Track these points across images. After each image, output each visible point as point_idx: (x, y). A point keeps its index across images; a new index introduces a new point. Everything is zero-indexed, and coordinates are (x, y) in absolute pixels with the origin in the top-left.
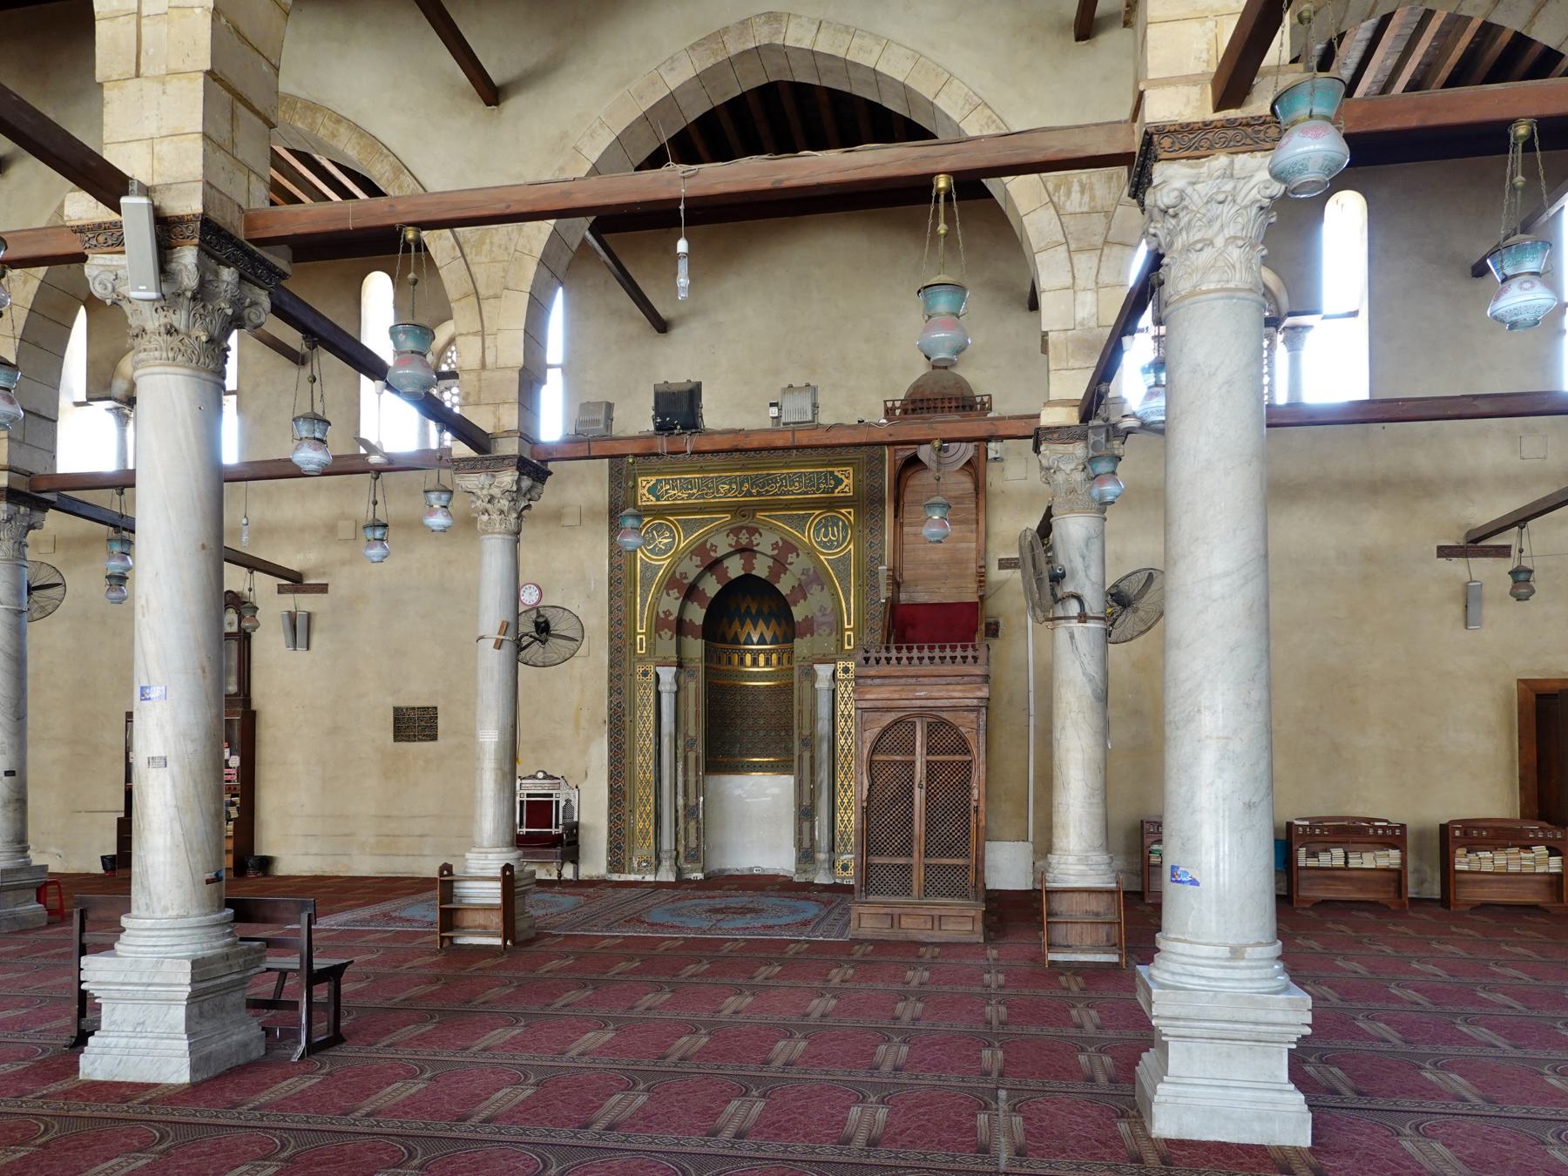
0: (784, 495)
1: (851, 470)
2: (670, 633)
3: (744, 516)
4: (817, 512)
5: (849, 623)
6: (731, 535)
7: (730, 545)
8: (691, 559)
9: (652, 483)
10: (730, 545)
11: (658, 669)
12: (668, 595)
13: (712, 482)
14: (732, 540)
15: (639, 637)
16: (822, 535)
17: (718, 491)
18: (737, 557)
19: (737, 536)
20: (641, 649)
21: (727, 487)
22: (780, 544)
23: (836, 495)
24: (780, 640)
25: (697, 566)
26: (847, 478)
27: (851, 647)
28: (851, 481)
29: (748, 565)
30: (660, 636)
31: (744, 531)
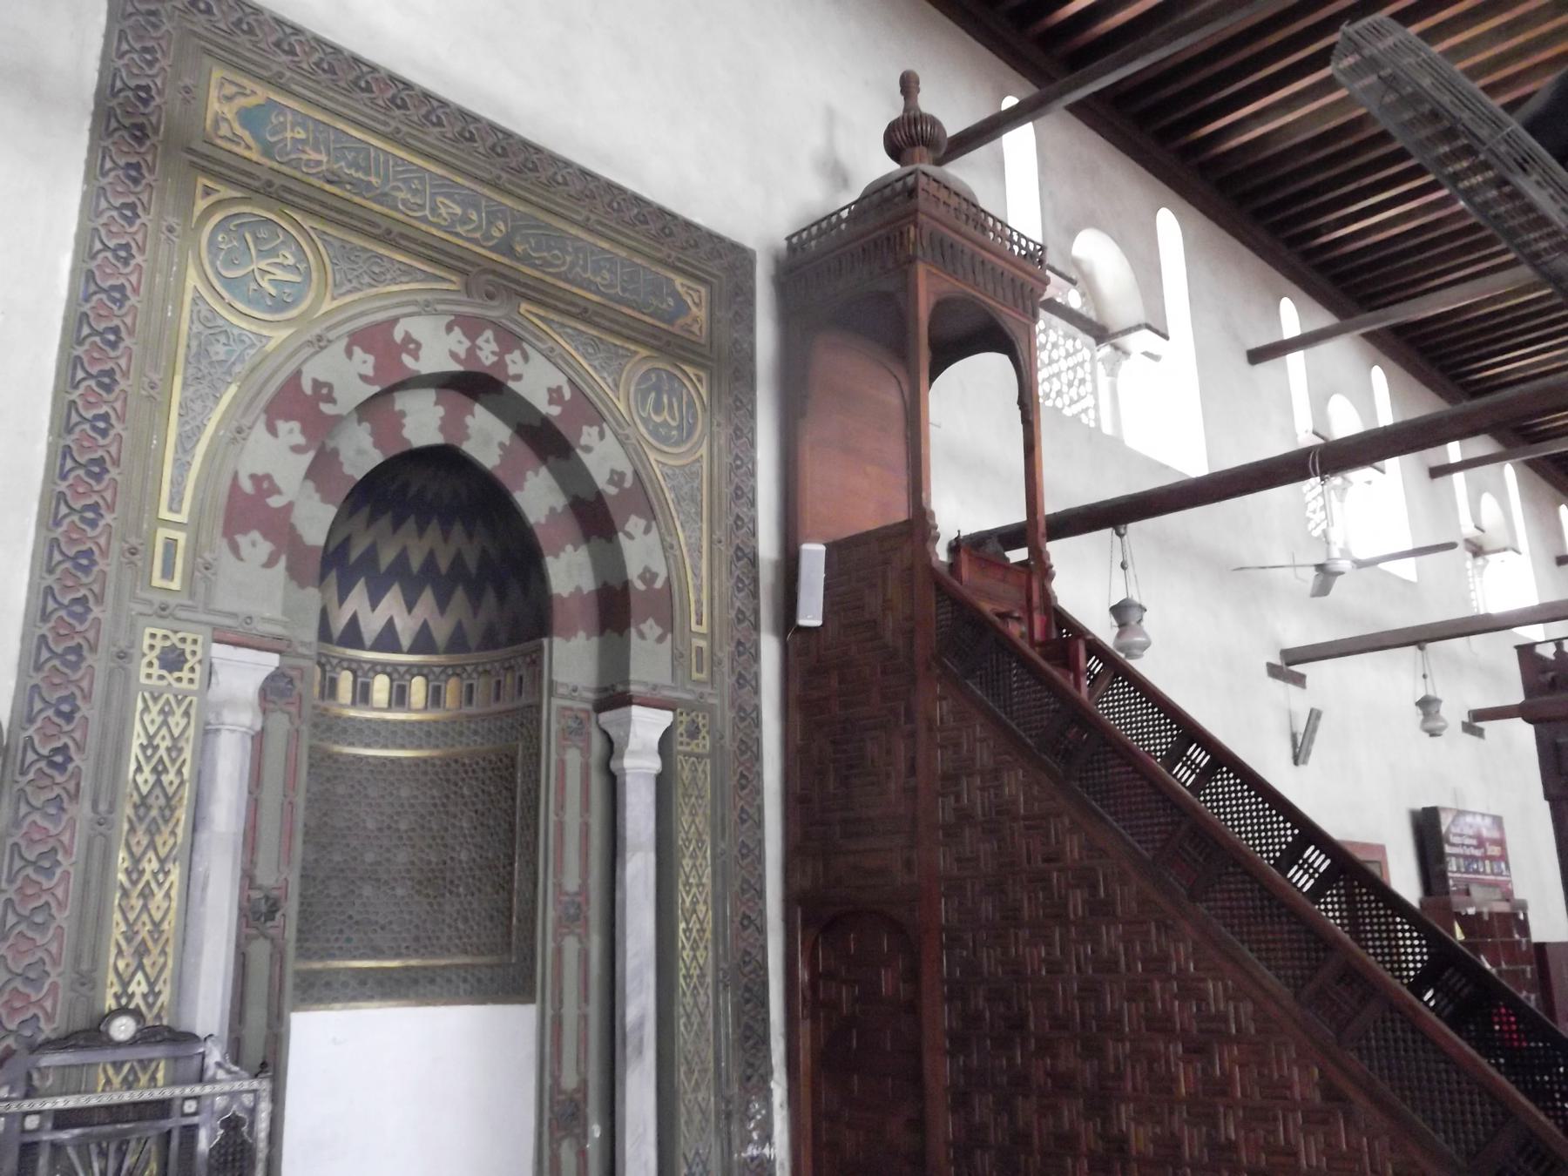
0: (581, 287)
1: (703, 290)
2: (265, 548)
3: (490, 296)
4: (644, 352)
5: (699, 622)
6: (457, 330)
7: (454, 355)
8: (349, 353)
9: (251, 101)
10: (454, 355)
11: (218, 651)
12: (272, 430)
13: (422, 180)
14: (457, 341)
15: (162, 534)
17: (434, 210)
18: (430, 395)
20: (168, 573)
21: (458, 210)
22: (567, 394)
23: (676, 330)
24: (406, 641)
25: (364, 378)
27: (704, 676)
28: (701, 313)
29: (452, 422)
30: (235, 549)
31: (489, 334)
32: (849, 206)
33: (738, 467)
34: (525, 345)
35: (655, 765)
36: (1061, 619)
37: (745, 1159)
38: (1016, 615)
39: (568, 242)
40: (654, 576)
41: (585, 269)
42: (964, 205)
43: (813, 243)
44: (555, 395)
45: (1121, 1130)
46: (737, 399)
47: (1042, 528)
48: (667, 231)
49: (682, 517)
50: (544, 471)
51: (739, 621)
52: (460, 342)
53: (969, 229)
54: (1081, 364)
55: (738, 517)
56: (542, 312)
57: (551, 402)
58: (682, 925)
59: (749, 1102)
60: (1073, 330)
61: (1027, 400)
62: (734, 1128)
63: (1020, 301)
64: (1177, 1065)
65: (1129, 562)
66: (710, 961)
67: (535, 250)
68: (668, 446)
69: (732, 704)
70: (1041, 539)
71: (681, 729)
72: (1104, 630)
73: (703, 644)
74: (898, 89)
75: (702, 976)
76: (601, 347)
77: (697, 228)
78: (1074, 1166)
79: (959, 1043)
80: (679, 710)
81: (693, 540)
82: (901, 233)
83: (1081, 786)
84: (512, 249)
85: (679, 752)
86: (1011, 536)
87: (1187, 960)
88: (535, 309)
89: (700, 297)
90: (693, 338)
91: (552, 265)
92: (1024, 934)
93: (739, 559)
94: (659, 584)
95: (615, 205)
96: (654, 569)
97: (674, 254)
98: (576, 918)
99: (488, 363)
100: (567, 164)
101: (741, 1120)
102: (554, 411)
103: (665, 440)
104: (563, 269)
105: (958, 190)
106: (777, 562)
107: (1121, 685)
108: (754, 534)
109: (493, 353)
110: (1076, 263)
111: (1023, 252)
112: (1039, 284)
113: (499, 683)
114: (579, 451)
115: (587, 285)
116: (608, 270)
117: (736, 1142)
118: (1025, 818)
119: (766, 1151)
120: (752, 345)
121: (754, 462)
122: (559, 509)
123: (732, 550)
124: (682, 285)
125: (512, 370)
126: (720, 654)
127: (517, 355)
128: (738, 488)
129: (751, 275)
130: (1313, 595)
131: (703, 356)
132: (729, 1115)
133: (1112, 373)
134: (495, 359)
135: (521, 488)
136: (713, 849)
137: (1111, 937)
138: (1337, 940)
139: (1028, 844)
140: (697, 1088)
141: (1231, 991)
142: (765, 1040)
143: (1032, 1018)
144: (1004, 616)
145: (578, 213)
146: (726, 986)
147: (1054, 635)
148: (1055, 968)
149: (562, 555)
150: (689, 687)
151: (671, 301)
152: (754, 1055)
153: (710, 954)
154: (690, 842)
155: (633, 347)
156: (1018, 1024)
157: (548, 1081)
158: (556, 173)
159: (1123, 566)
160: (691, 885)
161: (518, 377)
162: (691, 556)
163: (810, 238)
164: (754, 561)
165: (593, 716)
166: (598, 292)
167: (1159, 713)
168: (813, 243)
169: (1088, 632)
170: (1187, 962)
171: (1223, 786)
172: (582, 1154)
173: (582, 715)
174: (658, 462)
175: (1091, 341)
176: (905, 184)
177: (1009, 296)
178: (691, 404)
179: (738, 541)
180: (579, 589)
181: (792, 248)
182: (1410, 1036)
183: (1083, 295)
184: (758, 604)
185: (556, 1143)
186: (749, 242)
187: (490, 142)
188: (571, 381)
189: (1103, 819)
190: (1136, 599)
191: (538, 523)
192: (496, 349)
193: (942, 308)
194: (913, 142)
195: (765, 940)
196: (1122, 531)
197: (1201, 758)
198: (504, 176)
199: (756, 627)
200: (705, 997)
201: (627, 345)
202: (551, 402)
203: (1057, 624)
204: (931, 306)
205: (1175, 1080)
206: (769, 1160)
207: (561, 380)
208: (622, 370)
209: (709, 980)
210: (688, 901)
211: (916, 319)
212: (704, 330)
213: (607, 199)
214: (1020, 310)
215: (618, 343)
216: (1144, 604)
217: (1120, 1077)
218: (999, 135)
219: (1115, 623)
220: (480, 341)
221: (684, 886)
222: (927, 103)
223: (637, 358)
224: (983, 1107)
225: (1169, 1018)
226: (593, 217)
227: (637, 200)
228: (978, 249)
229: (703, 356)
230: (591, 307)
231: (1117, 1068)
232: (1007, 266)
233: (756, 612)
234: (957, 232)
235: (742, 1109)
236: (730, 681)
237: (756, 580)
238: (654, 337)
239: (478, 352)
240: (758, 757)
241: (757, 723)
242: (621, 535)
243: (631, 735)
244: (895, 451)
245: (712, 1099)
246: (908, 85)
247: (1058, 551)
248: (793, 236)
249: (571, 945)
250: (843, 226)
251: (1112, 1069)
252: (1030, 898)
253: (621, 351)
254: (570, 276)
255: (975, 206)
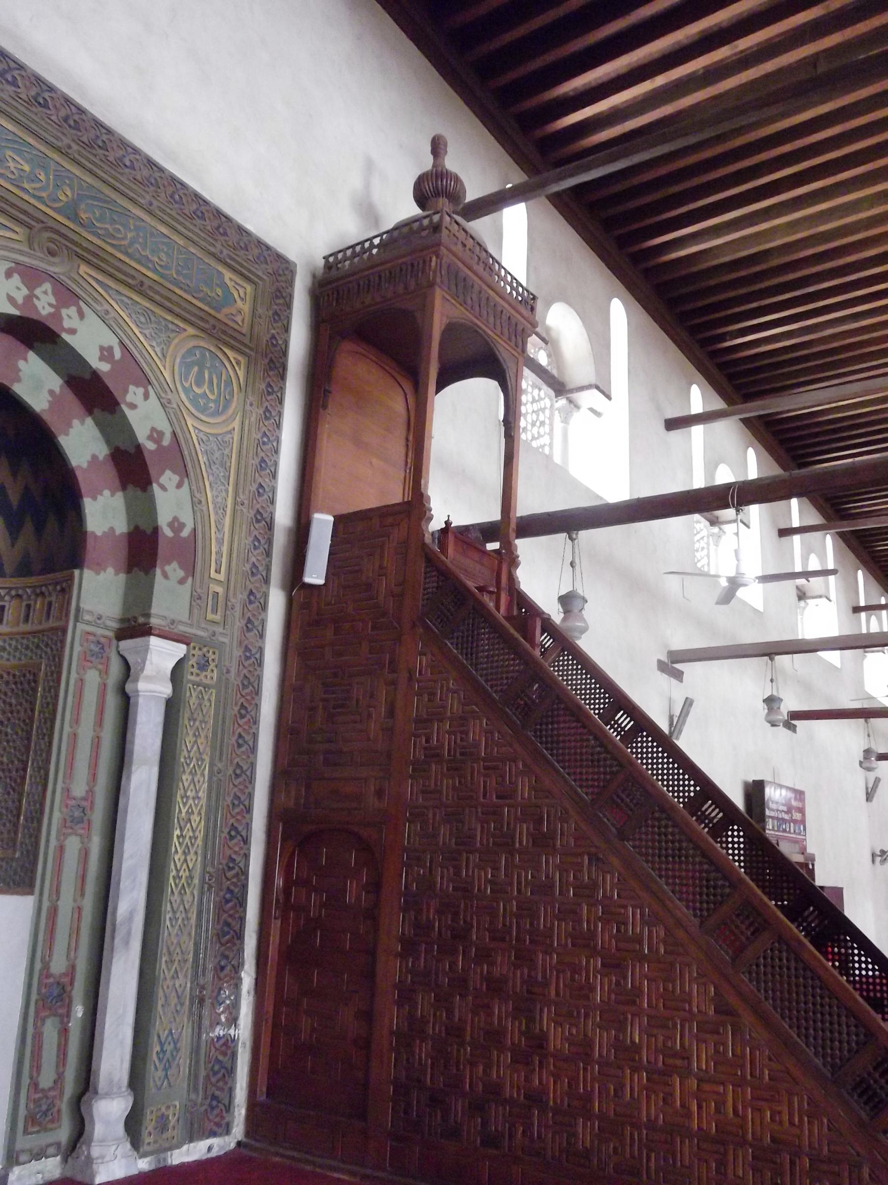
0: (139, 262)
1: (249, 288)
3: (52, 253)
4: (191, 331)
5: (218, 571)
7: (11, 300)
10: (11, 300)
16: (192, 377)
19: (31, 287)
22: (118, 354)
26: (242, 299)
27: (218, 617)
28: (246, 307)
31: (47, 286)
32: (380, 235)
33: (264, 443)
34: (81, 303)
35: (166, 690)
36: (521, 600)
37: (213, 1039)
38: (491, 589)
39: (131, 221)
40: (182, 526)
41: (144, 247)
42: (478, 248)
43: (347, 263)
44: (106, 353)
45: (541, 1030)
46: (269, 385)
47: (513, 525)
48: (221, 230)
49: (211, 478)
50: (89, 421)
51: (253, 574)
52: (18, 288)
53: (480, 269)
54: (543, 410)
55: (261, 486)
56: (100, 277)
57: (101, 359)
58: (177, 832)
59: (220, 989)
60: (539, 381)
61: (511, 419)
62: (206, 1012)
63: (513, 337)
64: (595, 977)
65: (577, 561)
66: (199, 866)
67: (98, 220)
68: (206, 415)
69: (240, 643)
70: (512, 534)
71: (193, 661)
72: (555, 613)
73: (220, 590)
74: (429, 148)
75: (191, 877)
76: (153, 318)
77: (248, 233)
78: (499, 1057)
79: (409, 947)
80: (192, 645)
81: (219, 500)
82: (424, 262)
83: (535, 736)
84: (77, 215)
85: (189, 681)
86: (489, 531)
87: (612, 890)
88: (93, 273)
89: (245, 294)
90: (236, 327)
91: (114, 237)
92: (475, 858)
93: (258, 521)
94: (185, 533)
95: (177, 197)
96: (182, 520)
97: (225, 252)
98: (81, 821)
99: (44, 312)
100: (136, 151)
101: (212, 1004)
102: (103, 367)
103: (203, 410)
104: (123, 243)
105: (474, 235)
106: (290, 530)
107: (566, 659)
108: (272, 502)
109: (50, 305)
110: (548, 329)
111: (520, 298)
112: (529, 326)
113: (28, 607)
114: (124, 407)
115: (143, 261)
116: (166, 253)
117: (206, 1022)
118: (484, 760)
119: (232, 1032)
120: (286, 343)
121: (278, 440)
122: (101, 458)
123: (252, 513)
124: (231, 279)
125: (67, 324)
126: (233, 600)
127: (72, 311)
128: (263, 460)
129: (291, 283)
130: (717, 603)
131: (245, 345)
132: (202, 1001)
133: (565, 421)
134: (52, 310)
135: (67, 434)
136: (212, 765)
137: (550, 864)
138: (741, 880)
139: (485, 783)
140: (175, 976)
141: (647, 918)
142: (240, 936)
143: (475, 930)
144: (481, 589)
145: (143, 197)
146: (210, 887)
147: (515, 613)
148: (499, 890)
149: (99, 497)
150: (203, 625)
151: (219, 291)
152: (229, 949)
153: (199, 859)
154: (191, 759)
155: (181, 325)
156: (461, 936)
157: (38, 966)
158: (124, 156)
159: (572, 564)
160: (188, 798)
161: (73, 332)
162: (216, 513)
163: (345, 259)
164: (270, 526)
165: (114, 642)
166: (155, 271)
167: (595, 683)
168: (347, 263)
169: (543, 613)
170: (612, 890)
171: (642, 747)
172: (64, 1032)
173: (103, 640)
174: (195, 428)
175: (552, 393)
176: (431, 221)
177: (506, 331)
178: (229, 382)
179: (258, 506)
180: (112, 529)
181: (328, 267)
182: (793, 964)
183: (549, 356)
184: (270, 562)
185: (40, 1020)
186: (292, 255)
187: (63, 113)
188: (122, 343)
189: (553, 766)
190: (580, 592)
191: (79, 467)
192: (54, 302)
193: (451, 330)
194: (437, 194)
195: (249, 849)
196: (574, 536)
197: (625, 721)
198: (75, 147)
199: (267, 581)
200: (192, 896)
201: (176, 322)
202: (101, 359)
203: (518, 604)
204: (443, 327)
205: (592, 989)
206: (233, 1040)
207: (111, 340)
208: (170, 343)
209: (196, 881)
210: (184, 811)
211: (430, 337)
212: (246, 321)
213: (170, 190)
214: (513, 344)
215: (169, 318)
216: (586, 597)
217: (546, 984)
218: (501, 209)
219: (561, 610)
220: (38, 292)
221: (182, 798)
222: (451, 163)
223: (184, 334)
224: (424, 1002)
225: (592, 934)
226: (155, 203)
227: (197, 197)
228: (485, 287)
229: (245, 345)
230: (147, 282)
231: (544, 976)
232: (506, 306)
233: (268, 569)
234: (470, 268)
235: (215, 994)
236: (239, 624)
237: (270, 542)
238: (202, 319)
239: (36, 301)
240: (257, 692)
241: (260, 663)
242: (155, 486)
243: (147, 662)
244: (396, 448)
245: (189, 985)
246: (437, 147)
247: (524, 546)
248: (331, 255)
249: (73, 845)
250: (375, 251)
251: (540, 978)
252: (482, 827)
253: (170, 326)
254: (130, 251)
255: (486, 251)
